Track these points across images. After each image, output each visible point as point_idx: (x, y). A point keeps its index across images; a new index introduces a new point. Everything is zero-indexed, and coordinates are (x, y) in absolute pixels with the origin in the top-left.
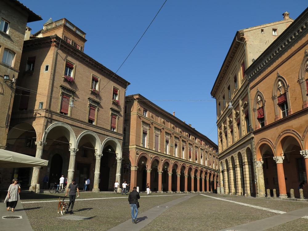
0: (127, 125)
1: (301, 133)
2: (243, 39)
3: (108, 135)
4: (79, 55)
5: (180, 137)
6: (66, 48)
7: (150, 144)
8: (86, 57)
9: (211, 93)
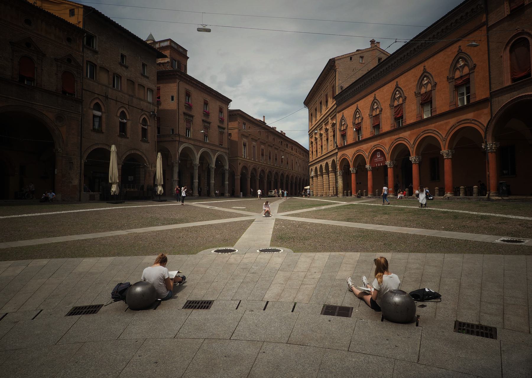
1: (367, 153)
9: (304, 103)
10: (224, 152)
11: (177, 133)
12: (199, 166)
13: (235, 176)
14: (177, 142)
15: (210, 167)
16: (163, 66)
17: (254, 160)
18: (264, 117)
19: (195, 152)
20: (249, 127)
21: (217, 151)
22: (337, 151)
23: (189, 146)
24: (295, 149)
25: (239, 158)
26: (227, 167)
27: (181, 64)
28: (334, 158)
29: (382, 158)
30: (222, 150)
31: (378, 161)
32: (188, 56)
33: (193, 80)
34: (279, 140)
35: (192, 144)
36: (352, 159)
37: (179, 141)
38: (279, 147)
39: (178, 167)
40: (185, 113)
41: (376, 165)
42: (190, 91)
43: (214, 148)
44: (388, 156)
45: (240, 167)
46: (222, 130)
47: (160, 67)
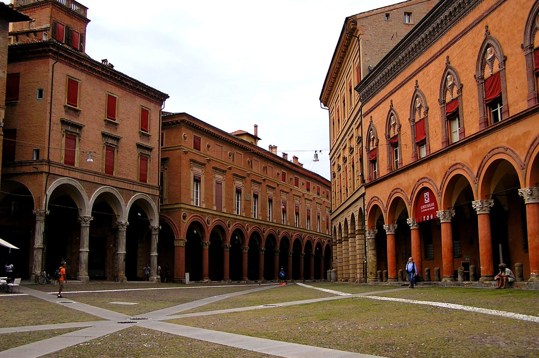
0: (166, 167)
2: (354, 30)
3: (135, 190)
4: (86, 64)
5: (264, 180)
6: (67, 57)
7: (207, 200)
8: (97, 66)
9: (320, 99)
10: (149, 194)
11: (46, 158)
12: (91, 222)
13: (175, 241)
15: (119, 223)
16: (35, 35)
17: (219, 209)
18: (256, 126)
19: (84, 194)
20: (208, 146)
21: (134, 191)
22: (363, 190)
23: (70, 183)
24: (314, 188)
25: (182, 206)
26: (155, 223)
27: (75, 33)
28: (360, 204)
29: (433, 204)
30: (146, 190)
31: (426, 210)
32: (88, 17)
33: (85, 60)
34: (277, 171)
36: (387, 206)
37: (49, 173)
38: (278, 185)
39: (44, 223)
41: (423, 217)
42: (78, 81)
44: (440, 200)
45: (185, 225)
46: (146, 152)
47: (28, 38)
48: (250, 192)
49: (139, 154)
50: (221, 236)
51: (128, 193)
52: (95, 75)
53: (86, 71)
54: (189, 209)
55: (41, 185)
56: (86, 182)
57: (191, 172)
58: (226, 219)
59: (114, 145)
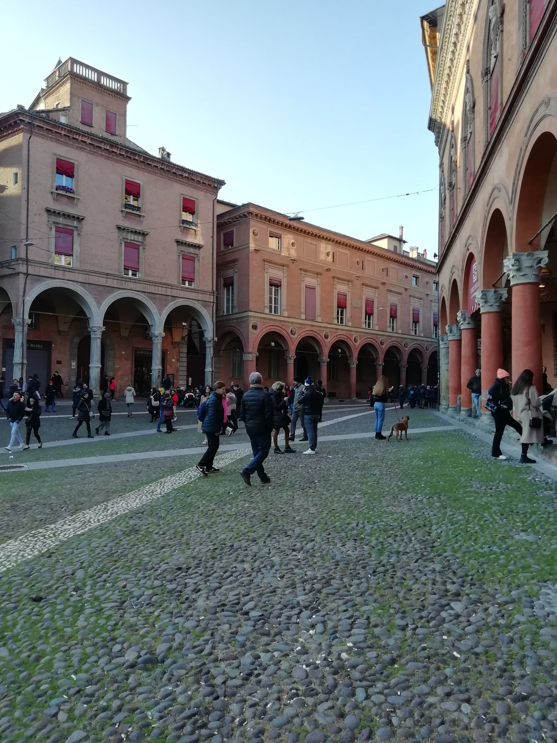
0: (236, 270)
5: (384, 284)
11: (23, 256)
14: (22, 277)
25: (250, 314)
32: (129, 94)
35: (77, 282)
37: (27, 274)
38: (406, 289)
40: (50, 211)
42: (73, 161)
43: (161, 290)
46: (192, 250)
48: (361, 298)
49: (179, 253)
50: (317, 348)
51: (165, 298)
52: (102, 155)
53: (85, 149)
54: (261, 318)
55: (18, 289)
56: (92, 286)
57: (266, 275)
58: (322, 329)
59: (139, 242)
